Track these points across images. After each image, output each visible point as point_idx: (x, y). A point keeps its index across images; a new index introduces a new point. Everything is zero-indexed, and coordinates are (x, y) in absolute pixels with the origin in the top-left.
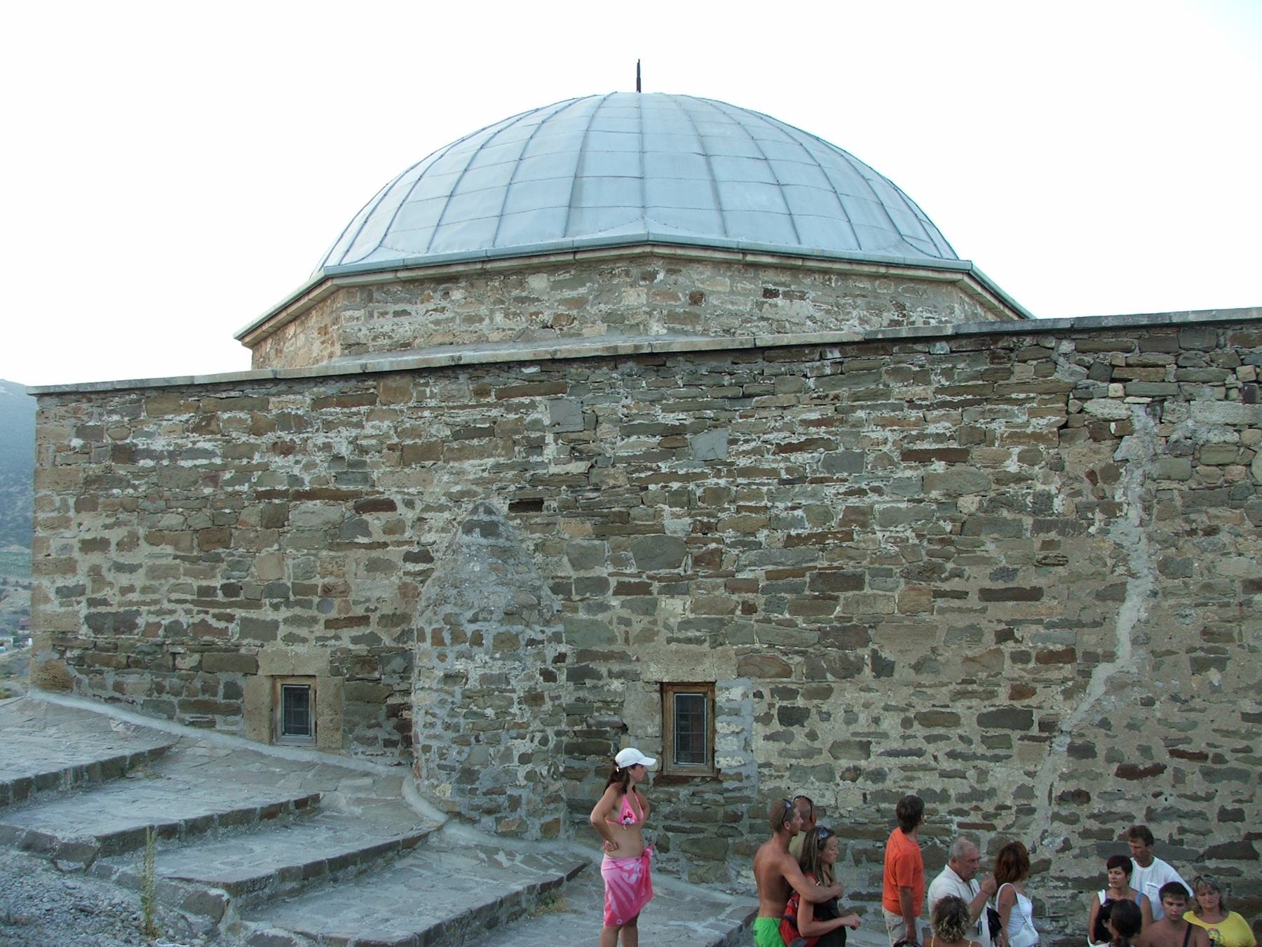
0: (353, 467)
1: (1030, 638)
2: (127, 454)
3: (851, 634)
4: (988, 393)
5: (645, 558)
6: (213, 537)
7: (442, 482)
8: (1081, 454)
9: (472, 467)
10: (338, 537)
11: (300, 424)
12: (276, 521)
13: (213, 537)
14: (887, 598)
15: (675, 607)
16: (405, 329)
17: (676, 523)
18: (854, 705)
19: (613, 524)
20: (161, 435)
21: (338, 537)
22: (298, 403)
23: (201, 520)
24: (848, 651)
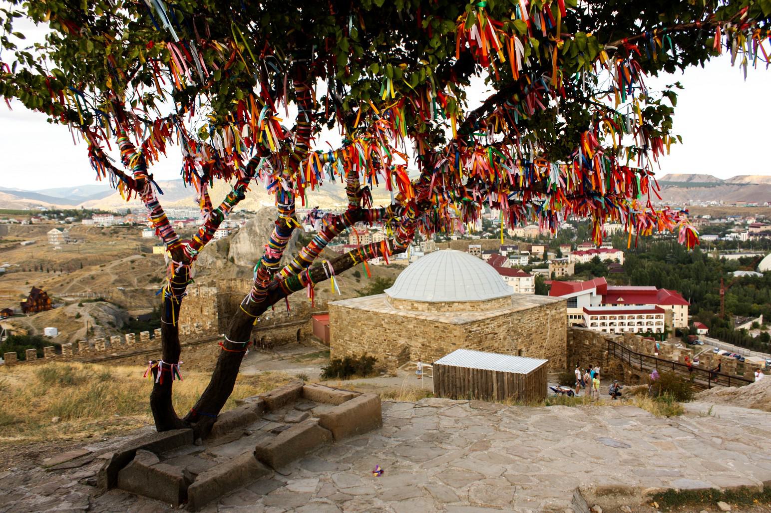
0: (494, 329)
1: (543, 337)
2: (470, 332)
3: (532, 340)
4: (540, 312)
5: (518, 335)
6: (480, 342)
7: (502, 329)
8: (546, 317)
9: (504, 327)
10: (493, 339)
11: (488, 324)
12: (486, 338)
13: (480, 342)
14: (533, 336)
15: (520, 340)
16: (488, 307)
17: (520, 331)
18: (532, 347)
19: (515, 332)
20: (474, 328)
21: (493, 339)
22: (488, 321)
23: (479, 339)
24: (531, 343)
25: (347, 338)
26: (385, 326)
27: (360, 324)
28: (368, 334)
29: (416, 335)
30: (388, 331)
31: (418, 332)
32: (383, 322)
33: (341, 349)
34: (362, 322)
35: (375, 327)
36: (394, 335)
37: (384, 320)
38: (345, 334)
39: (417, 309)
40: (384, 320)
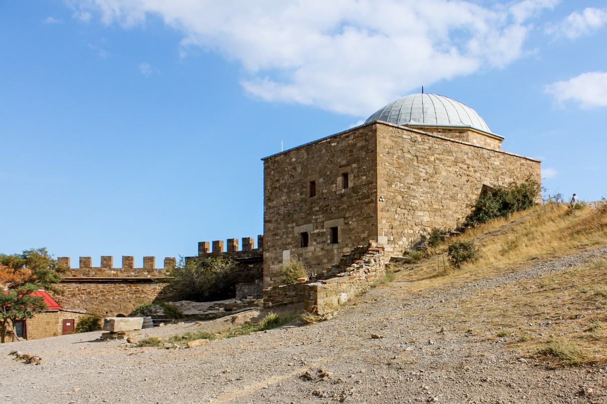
25: (410, 180)
26: (468, 162)
27: (432, 159)
28: (444, 173)
29: (502, 174)
30: (471, 169)
31: (504, 170)
32: (465, 157)
33: (399, 198)
34: (436, 156)
35: (456, 163)
36: (478, 175)
37: (467, 154)
38: (407, 174)
39: (490, 145)
40: (467, 154)
